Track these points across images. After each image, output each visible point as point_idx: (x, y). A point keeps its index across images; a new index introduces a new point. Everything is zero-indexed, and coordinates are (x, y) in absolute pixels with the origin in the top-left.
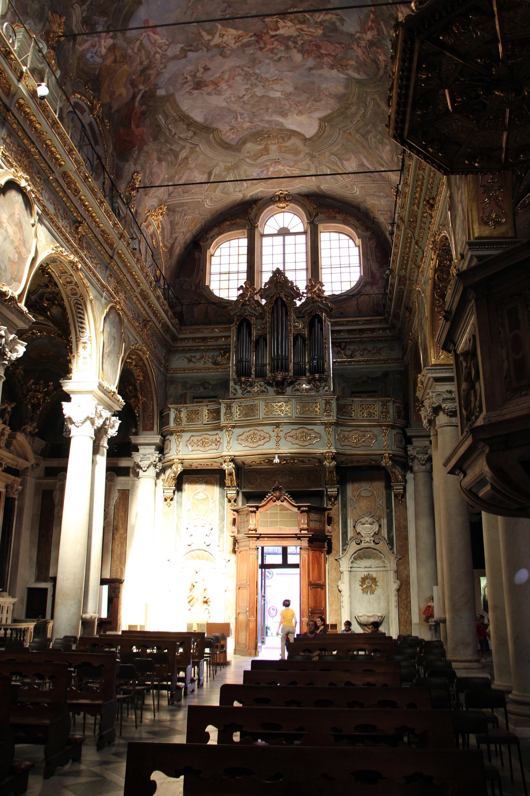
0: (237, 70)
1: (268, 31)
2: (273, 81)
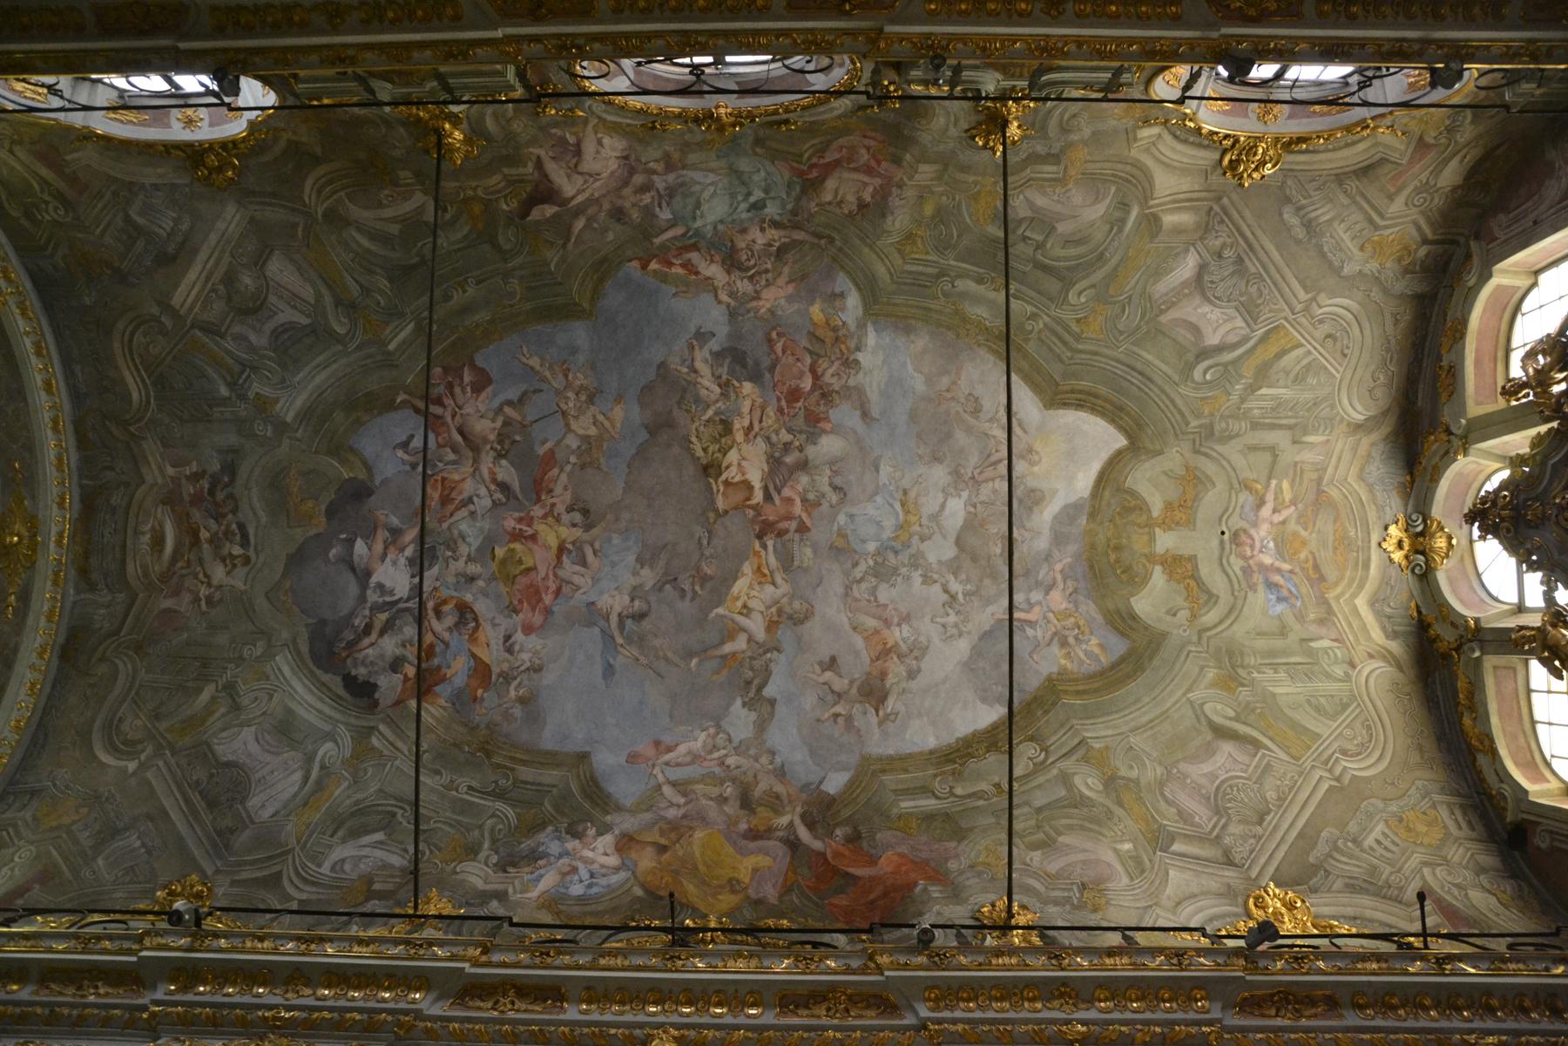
0: (856, 593)
1: (749, 507)
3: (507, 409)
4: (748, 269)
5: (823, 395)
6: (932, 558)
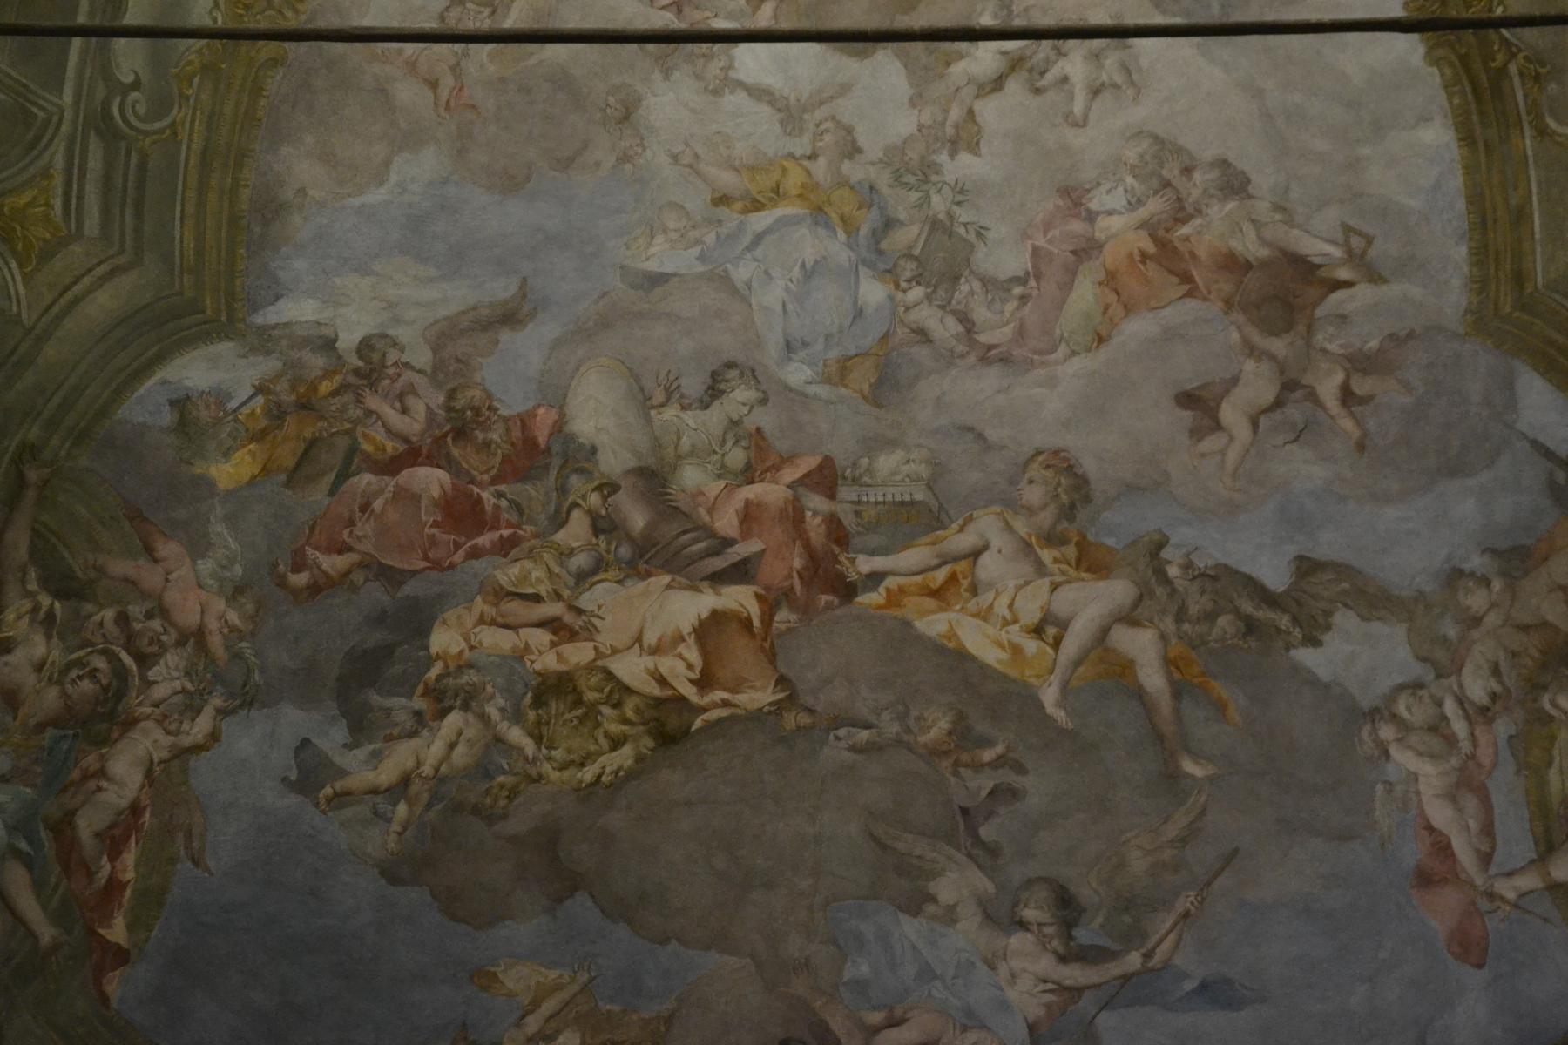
0: (999, 335)
1: (768, 619)
2: (777, 193)
4: (120, 673)
5: (461, 433)
6: (903, 124)
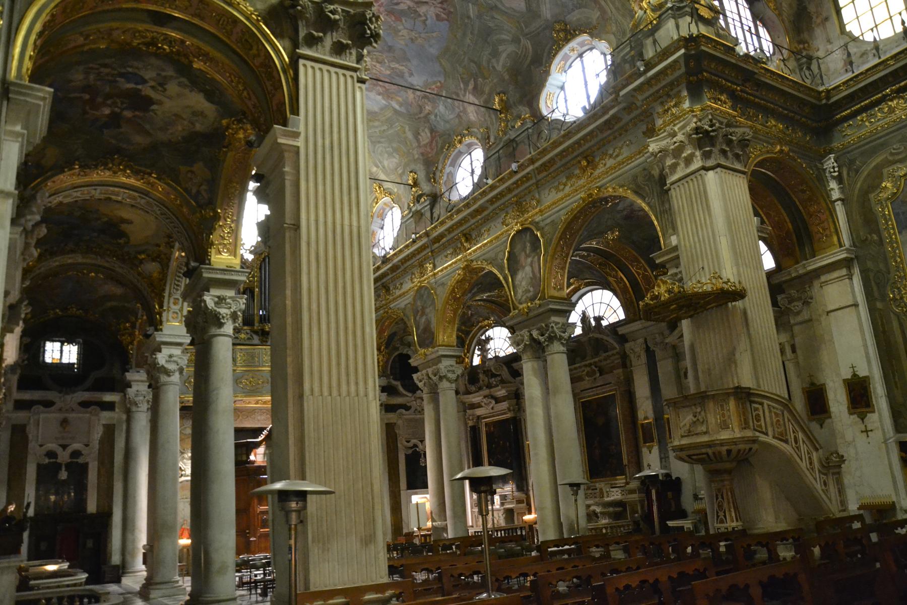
3: (424, 18)
